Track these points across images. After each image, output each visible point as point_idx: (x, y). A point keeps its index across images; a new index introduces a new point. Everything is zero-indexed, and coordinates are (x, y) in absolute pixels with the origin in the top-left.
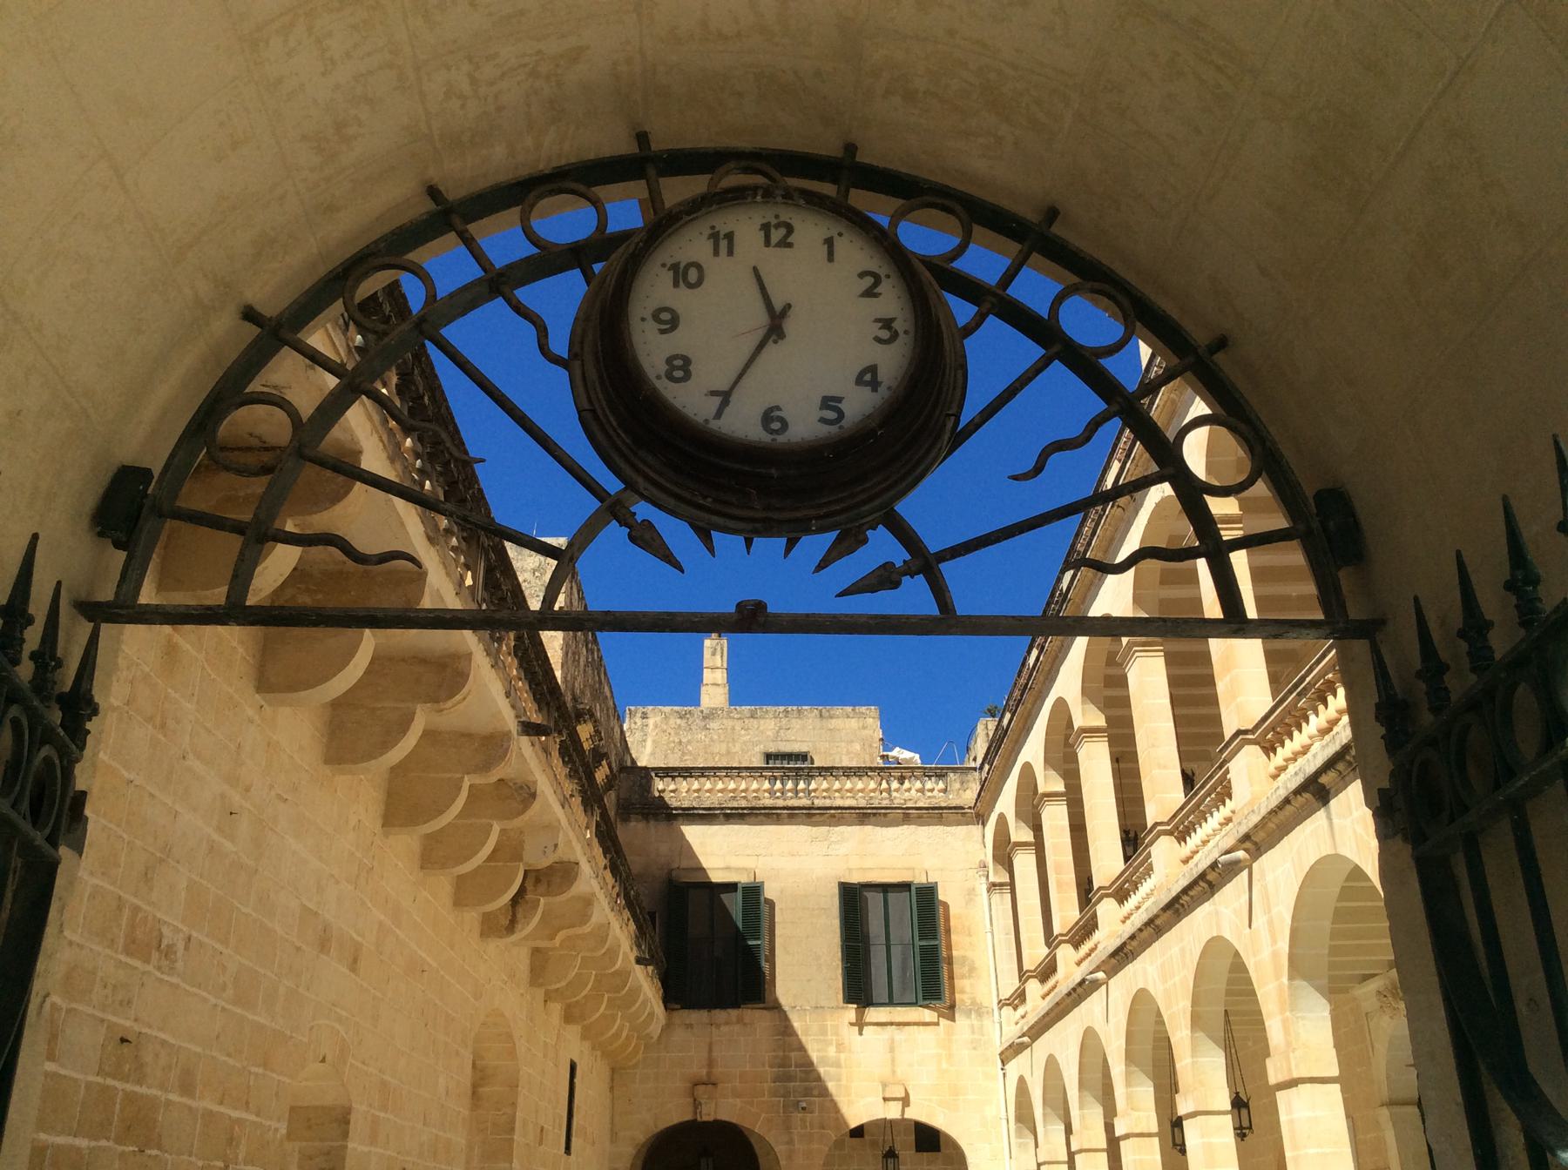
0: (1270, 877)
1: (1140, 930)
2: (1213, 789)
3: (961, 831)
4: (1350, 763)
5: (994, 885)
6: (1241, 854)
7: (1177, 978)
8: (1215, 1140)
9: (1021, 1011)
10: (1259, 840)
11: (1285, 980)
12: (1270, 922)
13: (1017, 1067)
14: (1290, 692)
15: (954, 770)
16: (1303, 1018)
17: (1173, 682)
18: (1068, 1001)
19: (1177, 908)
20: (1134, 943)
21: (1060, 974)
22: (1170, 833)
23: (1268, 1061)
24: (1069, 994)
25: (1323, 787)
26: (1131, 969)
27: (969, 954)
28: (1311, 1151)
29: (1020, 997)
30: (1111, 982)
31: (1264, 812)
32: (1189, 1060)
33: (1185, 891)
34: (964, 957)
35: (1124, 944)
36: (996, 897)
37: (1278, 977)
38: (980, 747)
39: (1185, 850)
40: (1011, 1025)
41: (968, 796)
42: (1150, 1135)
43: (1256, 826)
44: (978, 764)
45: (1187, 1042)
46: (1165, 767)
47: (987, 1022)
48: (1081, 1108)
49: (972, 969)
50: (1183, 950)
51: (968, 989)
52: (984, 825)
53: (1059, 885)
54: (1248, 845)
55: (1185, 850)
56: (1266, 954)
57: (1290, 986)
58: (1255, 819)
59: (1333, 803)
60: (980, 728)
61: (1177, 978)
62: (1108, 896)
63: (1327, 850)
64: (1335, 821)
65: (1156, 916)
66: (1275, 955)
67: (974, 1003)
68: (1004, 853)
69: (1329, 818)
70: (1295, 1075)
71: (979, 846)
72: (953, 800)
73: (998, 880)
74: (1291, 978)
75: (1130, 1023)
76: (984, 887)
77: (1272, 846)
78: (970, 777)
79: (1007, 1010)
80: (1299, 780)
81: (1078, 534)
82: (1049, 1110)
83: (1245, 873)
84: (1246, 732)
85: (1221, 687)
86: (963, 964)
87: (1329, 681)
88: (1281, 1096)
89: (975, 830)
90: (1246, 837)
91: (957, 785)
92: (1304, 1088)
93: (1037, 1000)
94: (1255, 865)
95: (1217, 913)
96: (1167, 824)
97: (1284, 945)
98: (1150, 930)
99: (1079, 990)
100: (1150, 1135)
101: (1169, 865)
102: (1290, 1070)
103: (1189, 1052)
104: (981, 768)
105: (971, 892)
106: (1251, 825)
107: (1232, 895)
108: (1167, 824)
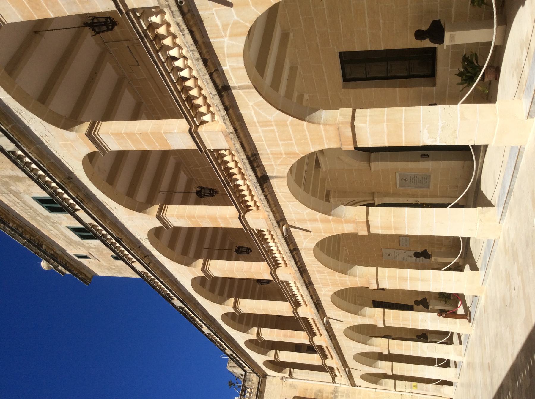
0: (293, 216)
1: (309, 292)
2: (260, 242)
3: (268, 385)
4: (254, 160)
5: (290, 375)
6: (284, 227)
7: (328, 278)
8: (387, 275)
9: (337, 372)
10: (281, 220)
11: (331, 218)
12: (310, 220)
13: (358, 381)
14: (227, 189)
15: (244, 383)
16: (345, 215)
17: (220, 258)
18: (334, 342)
19: (302, 270)
20: (314, 298)
21: (324, 345)
22: (275, 270)
23: (360, 234)
24: (332, 341)
25: (261, 177)
26: (323, 303)
27: (314, 391)
28: (392, 220)
29: (331, 370)
30: (328, 315)
31: (269, 210)
32: (357, 279)
33: (296, 263)
34: (315, 394)
35: (314, 302)
36: (294, 375)
37: (328, 221)
38: (238, 371)
39: (283, 265)
40: (342, 378)
41: (255, 378)
42: (384, 312)
43: (274, 216)
44: (243, 373)
45: (351, 278)
46: (251, 267)
47: (340, 390)
48: (373, 345)
49: (320, 391)
50: (318, 272)
51: (327, 395)
52: (267, 375)
53: (291, 337)
54: (281, 223)
55: (283, 265)
56: (321, 225)
57: (333, 216)
58: (271, 215)
59: (269, 174)
60: (230, 369)
61: (328, 278)
62: (296, 310)
63: (285, 181)
64: (275, 175)
65: (305, 282)
66: (322, 221)
67: (332, 394)
68: (278, 366)
69: (273, 177)
70: (365, 220)
71: (275, 379)
72: (255, 386)
73: (288, 373)
74: (330, 215)
75: (343, 310)
76: (290, 380)
77: (282, 212)
78: (248, 377)
79: (336, 380)
80: (258, 185)
81: (159, 292)
82: (373, 365)
83: (292, 230)
84: (240, 216)
85: (223, 225)
86: (318, 395)
87: (225, 169)
88: (373, 231)
89: (268, 379)
90: (278, 222)
91: (250, 383)
92: (370, 218)
93: (333, 362)
94: (289, 223)
95: (305, 249)
96: (272, 270)
97: (319, 215)
98: (309, 287)
99: (330, 334)
100: (384, 312)
101: (287, 273)
102: (363, 222)
103: (355, 278)
104: (245, 371)
105: (292, 386)
106: (273, 218)
107: (299, 238)
108: (272, 270)
